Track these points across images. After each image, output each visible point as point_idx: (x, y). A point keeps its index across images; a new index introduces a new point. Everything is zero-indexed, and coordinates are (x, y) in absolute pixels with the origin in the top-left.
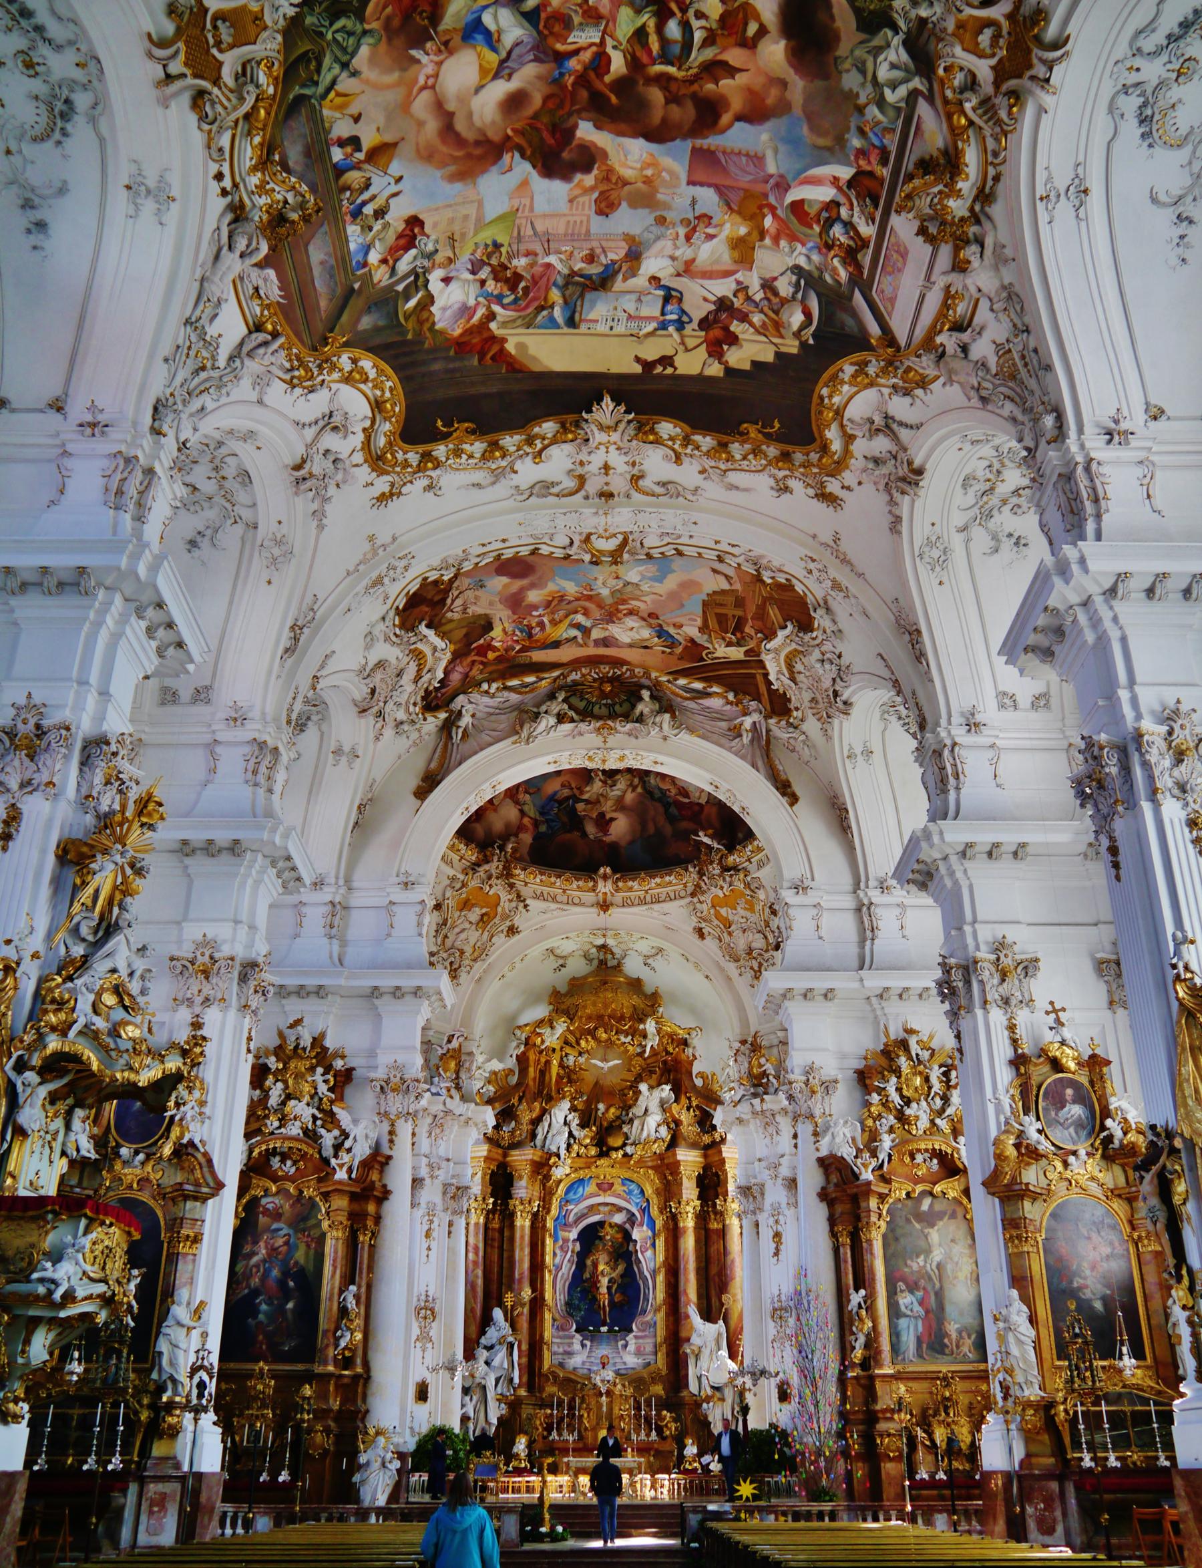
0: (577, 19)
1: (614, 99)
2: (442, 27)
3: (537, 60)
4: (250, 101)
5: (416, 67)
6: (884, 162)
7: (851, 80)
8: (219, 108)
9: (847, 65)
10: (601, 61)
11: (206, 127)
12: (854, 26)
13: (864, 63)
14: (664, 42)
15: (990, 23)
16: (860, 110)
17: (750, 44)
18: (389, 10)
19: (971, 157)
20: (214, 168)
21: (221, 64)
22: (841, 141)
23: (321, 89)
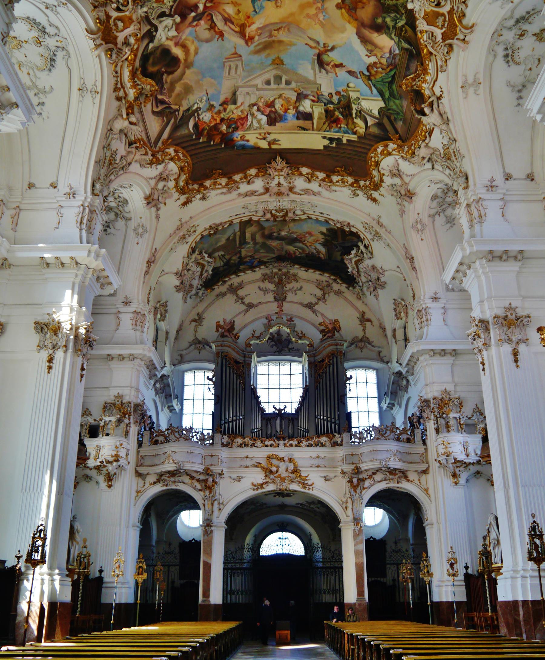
15: (122, 31)
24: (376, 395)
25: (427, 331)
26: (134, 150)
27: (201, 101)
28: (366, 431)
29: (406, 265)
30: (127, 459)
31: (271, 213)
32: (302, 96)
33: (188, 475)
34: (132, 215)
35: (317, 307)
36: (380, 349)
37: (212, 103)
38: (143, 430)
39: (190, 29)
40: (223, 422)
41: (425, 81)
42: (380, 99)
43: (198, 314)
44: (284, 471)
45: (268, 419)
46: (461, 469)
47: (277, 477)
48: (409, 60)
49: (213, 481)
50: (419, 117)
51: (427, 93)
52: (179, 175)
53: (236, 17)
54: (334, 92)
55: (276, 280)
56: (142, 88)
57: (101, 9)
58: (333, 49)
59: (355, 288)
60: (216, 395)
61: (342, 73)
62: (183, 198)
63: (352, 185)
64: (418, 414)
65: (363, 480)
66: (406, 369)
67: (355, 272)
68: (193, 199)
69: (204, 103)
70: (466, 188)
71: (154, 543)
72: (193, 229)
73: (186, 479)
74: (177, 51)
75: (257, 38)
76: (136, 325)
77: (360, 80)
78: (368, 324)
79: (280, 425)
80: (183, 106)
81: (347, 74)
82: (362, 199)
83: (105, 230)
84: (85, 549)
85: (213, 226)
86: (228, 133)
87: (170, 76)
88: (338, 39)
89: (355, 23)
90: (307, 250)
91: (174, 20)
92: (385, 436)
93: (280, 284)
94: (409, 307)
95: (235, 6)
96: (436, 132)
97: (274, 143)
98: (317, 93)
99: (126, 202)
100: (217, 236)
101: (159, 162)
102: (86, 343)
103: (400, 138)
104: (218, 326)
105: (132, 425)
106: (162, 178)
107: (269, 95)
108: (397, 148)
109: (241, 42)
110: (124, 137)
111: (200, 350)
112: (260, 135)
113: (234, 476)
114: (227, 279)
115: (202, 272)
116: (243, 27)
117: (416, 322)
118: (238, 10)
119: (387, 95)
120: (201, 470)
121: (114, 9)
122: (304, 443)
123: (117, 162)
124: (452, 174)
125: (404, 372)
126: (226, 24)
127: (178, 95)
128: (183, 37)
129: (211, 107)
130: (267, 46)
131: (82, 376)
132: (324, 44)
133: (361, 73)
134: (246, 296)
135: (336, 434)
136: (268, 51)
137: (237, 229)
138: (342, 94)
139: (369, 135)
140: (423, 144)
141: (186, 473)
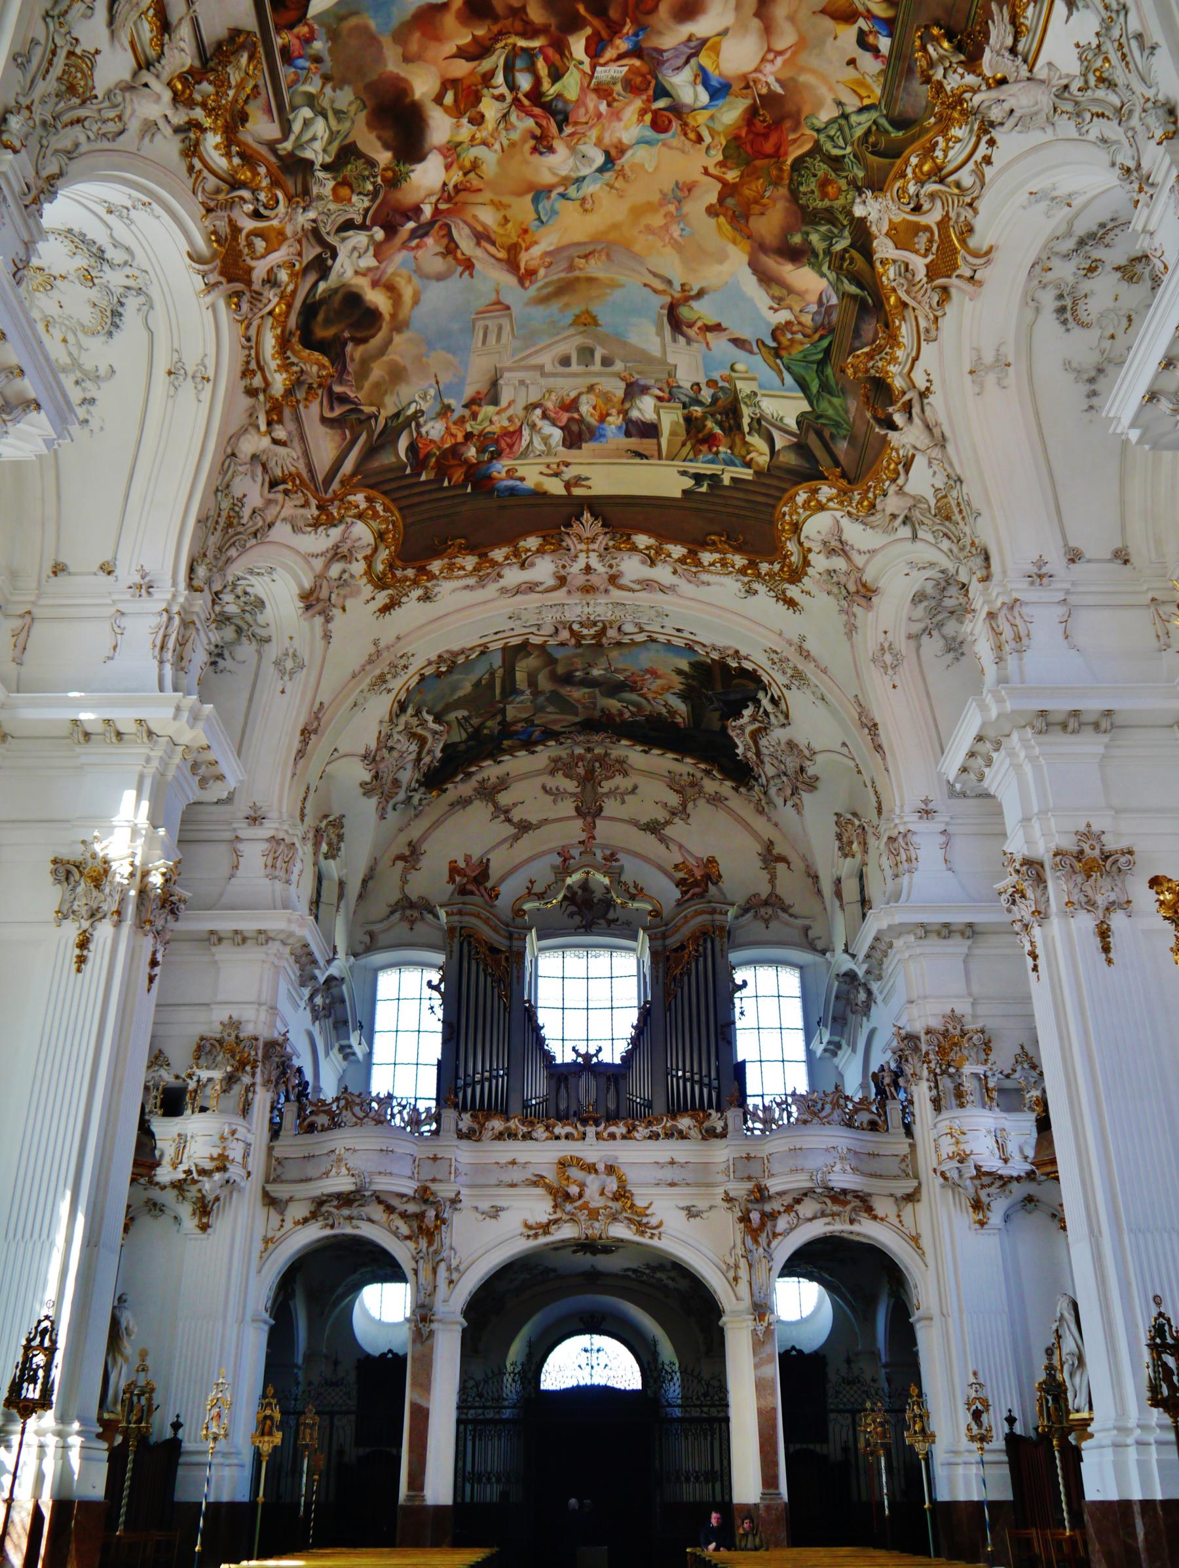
0: (618, 88)
1: (581, 9)
2: (748, 102)
3: (661, 52)
5: (782, 76)
7: (345, 98)
9: (353, 108)
10: (595, 49)
12: (360, 145)
13: (339, 120)
14: (532, 69)
15: (263, 257)
16: (326, 78)
17: (448, 84)
18: (792, 137)
20: (989, 171)
22: (333, 36)
23: (874, 115)
24: (800, 1024)
25: (910, 883)
26: (280, 497)
27: (424, 398)
28: (778, 1105)
29: (861, 740)
30: (244, 1166)
31: (571, 629)
32: (636, 389)
33: (380, 1201)
34: (272, 631)
35: (668, 831)
36: (807, 922)
37: (446, 401)
38: (282, 1100)
39: (404, 253)
40: (461, 1083)
41: (894, 360)
42: (801, 395)
43: (410, 844)
44: (597, 1196)
45: (562, 1075)
46: (993, 1190)
47: (580, 1208)
48: (860, 318)
49: (437, 1217)
50: (883, 432)
51: (898, 383)
52: (375, 550)
53: (500, 231)
54: (703, 381)
55: (581, 771)
56: (302, 371)
57: (220, 213)
58: (701, 294)
59: (751, 789)
60: (446, 1022)
61: (720, 345)
62: (382, 597)
63: (742, 571)
64: (893, 1065)
65: (773, 1216)
66: (865, 967)
67: (749, 754)
68: (404, 599)
69: (431, 401)
70: (986, 579)
71: (300, 1360)
72: (403, 662)
73: (377, 1212)
74: (377, 298)
75: (542, 272)
76: (274, 866)
77: (759, 358)
78: (781, 867)
79: (587, 1091)
80: (385, 407)
81: (731, 346)
82: (764, 602)
83: (214, 663)
84: (142, 1374)
85: (446, 656)
86: (479, 463)
87: (361, 348)
88: (710, 275)
89: (746, 244)
90: (648, 709)
91: (371, 237)
92: (824, 1114)
93: (589, 780)
94: (869, 830)
95: (498, 210)
96: (919, 463)
97: (576, 485)
98: (668, 383)
99: (260, 604)
100: (455, 677)
101: (332, 523)
102: (163, 907)
103: (844, 475)
104: (454, 870)
105: (258, 1088)
106: (337, 554)
107: (567, 386)
108: (838, 496)
109: (510, 280)
110: (259, 470)
111: (412, 922)
112: (548, 466)
113: (485, 1205)
114: (473, 769)
115: (419, 753)
116: (513, 250)
117: (885, 863)
118: (505, 217)
119: (815, 387)
120: (411, 1193)
121: (248, 215)
122: (642, 1131)
123: (244, 521)
124: (955, 550)
125: (860, 973)
126: (478, 244)
127: (377, 385)
128: (390, 270)
129: (446, 410)
130: (563, 289)
131: (151, 979)
132: (683, 285)
133: (760, 342)
134: (515, 805)
135: (712, 1112)
136: (565, 299)
137: (497, 661)
138: (721, 384)
139: (779, 468)
140: (893, 489)
141: (378, 1198)
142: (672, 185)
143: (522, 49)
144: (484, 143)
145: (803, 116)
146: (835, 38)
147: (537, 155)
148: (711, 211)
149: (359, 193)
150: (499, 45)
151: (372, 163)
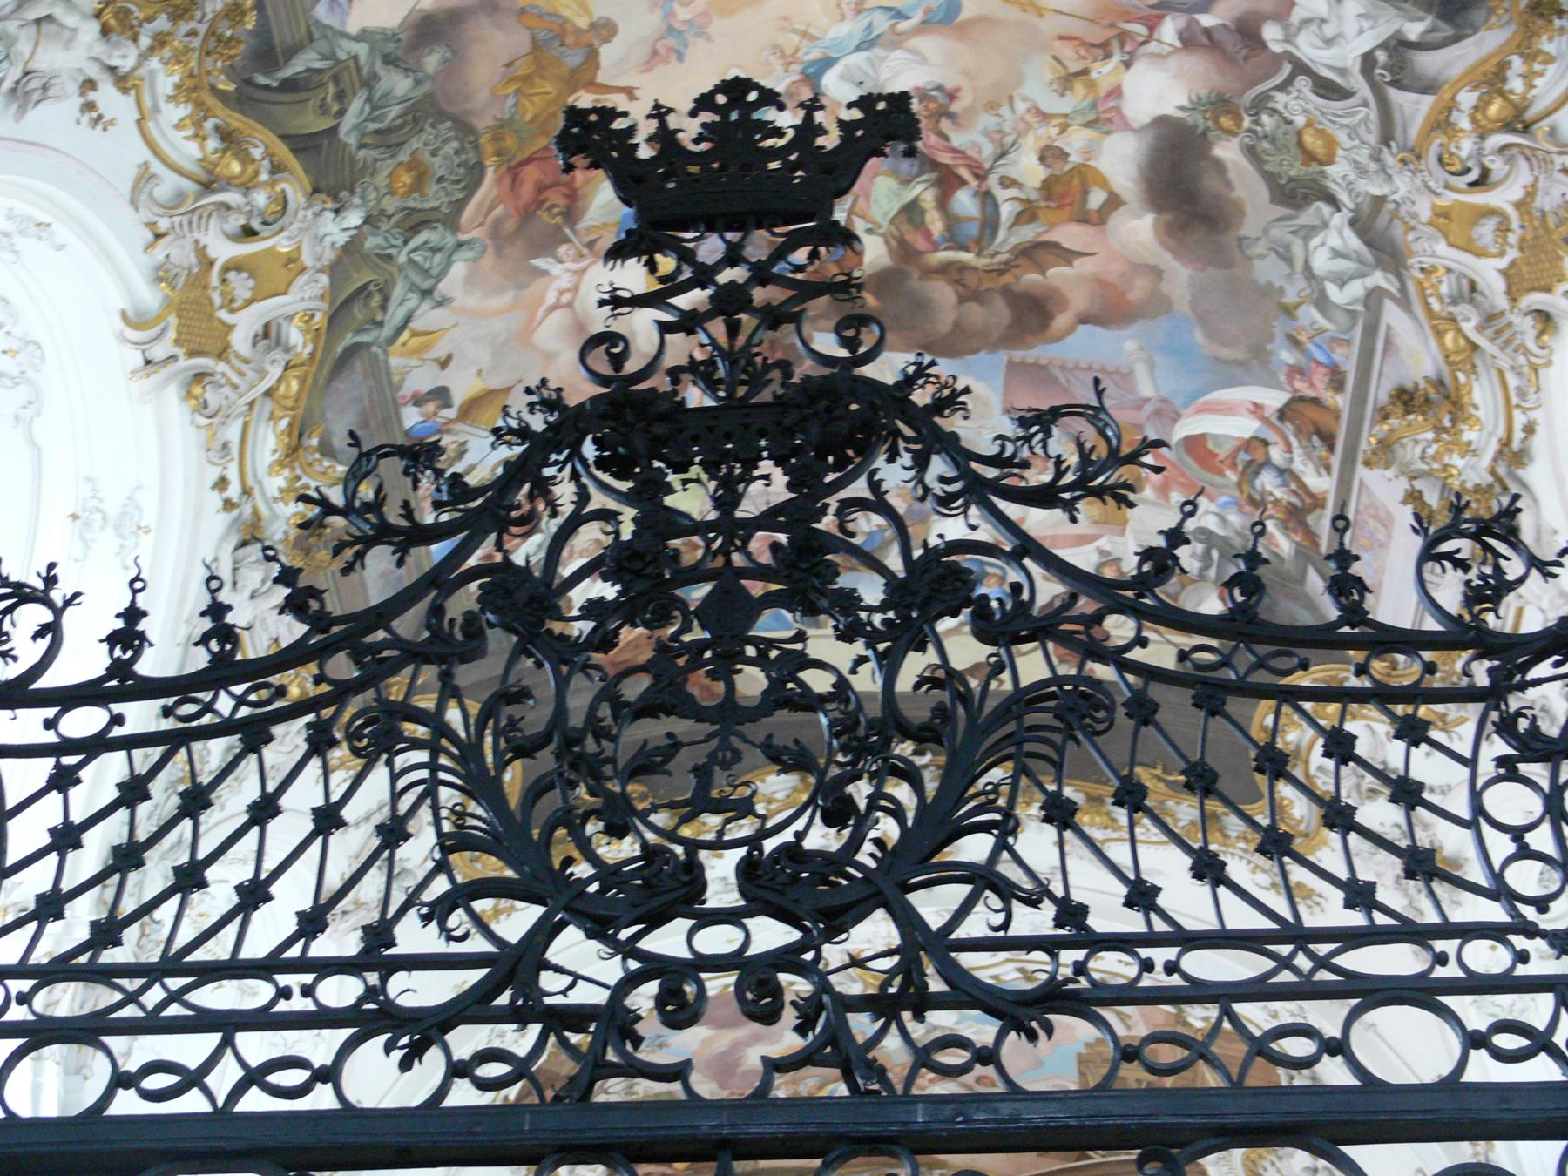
2: (581, 226)
4: (275, 372)
5: (544, 280)
6: (1338, 384)
8: (227, 390)
9: (1259, 249)
11: (205, 421)
13: (1287, 247)
14: (952, 221)
15: (1491, 212)
16: (1289, 311)
17: (1098, 219)
18: (498, 211)
19: (1482, 394)
20: (213, 474)
21: (230, 328)
23: (387, 331)
142: (690, 53)
143: (966, 249)
144: (1045, 117)
145: (490, 250)
146: (479, 373)
147: (949, 85)
148: (606, 30)
149: (1290, 123)
150: (1006, 256)
151: (1251, 152)
